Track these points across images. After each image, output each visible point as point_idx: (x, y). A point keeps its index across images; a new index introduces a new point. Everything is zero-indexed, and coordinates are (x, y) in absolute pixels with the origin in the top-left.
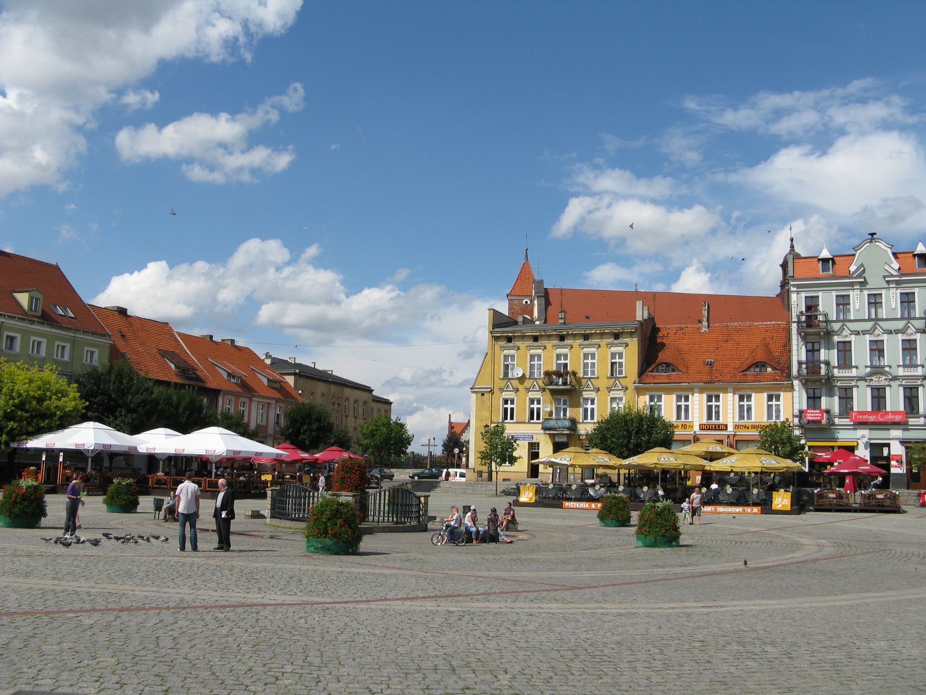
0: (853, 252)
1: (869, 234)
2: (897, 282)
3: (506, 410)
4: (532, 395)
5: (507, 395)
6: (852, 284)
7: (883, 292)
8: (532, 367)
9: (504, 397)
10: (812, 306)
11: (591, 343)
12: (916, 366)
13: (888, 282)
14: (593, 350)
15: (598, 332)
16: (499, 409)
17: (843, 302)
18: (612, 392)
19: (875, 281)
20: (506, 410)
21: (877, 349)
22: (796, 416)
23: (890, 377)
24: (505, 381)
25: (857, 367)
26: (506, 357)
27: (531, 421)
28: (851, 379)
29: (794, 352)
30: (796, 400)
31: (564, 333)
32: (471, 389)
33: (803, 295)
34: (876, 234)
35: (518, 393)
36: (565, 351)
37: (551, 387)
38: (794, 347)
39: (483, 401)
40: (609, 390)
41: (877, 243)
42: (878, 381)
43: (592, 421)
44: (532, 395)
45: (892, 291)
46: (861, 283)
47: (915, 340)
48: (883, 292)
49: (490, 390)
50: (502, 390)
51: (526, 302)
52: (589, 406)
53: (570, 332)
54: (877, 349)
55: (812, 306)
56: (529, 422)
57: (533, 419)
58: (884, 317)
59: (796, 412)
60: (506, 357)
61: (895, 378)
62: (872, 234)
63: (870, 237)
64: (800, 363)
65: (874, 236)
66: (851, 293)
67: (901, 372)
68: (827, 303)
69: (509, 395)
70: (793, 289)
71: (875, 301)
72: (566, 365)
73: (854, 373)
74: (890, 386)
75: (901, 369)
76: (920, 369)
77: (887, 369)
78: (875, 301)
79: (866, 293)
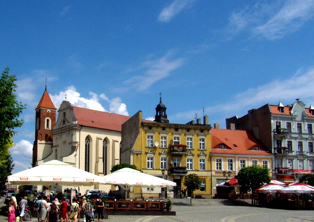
1: (296, 100)
2: (307, 119)
3: (148, 163)
10: (278, 126)
17: (289, 125)
20: (148, 163)
21: (300, 145)
28: (293, 156)
29: (273, 144)
30: (274, 164)
34: (299, 99)
36: (178, 136)
38: (273, 142)
39: (138, 158)
40: (199, 156)
43: (191, 170)
54: (300, 145)
55: (278, 126)
62: (297, 100)
63: (297, 100)
65: (299, 100)
67: (308, 155)
68: (284, 125)
69: (151, 155)
71: (299, 126)
72: (178, 142)
73: (294, 154)
77: (304, 153)
79: (296, 122)
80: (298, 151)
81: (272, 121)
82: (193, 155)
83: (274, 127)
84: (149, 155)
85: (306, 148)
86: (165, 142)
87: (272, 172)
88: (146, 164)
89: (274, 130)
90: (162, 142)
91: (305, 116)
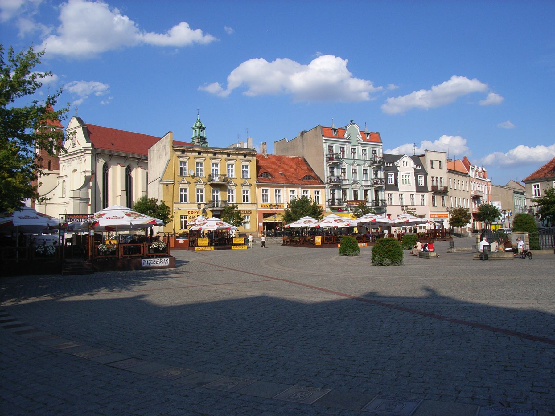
0: (345, 128)
4: (198, 186)
5: (182, 186)
6: (346, 142)
7: (356, 147)
8: (197, 169)
9: (181, 187)
11: (231, 158)
12: (368, 181)
13: (358, 143)
14: (232, 162)
15: (237, 152)
16: (178, 195)
18: (243, 187)
19: (354, 142)
22: (327, 202)
23: (360, 185)
24: (181, 178)
25: (348, 180)
26: (181, 163)
27: (181, 202)
28: (346, 185)
29: (325, 171)
31: (218, 151)
32: (161, 181)
33: (328, 145)
35: (190, 185)
37: (211, 183)
38: (325, 169)
40: (242, 185)
41: (354, 125)
42: (356, 186)
44: (198, 186)
45: (359, 147)
46: (349, 142)
47: (345, 169)
48: (356, 147)
49: (173, 183)
50: (180, 183)
51: (53, 130)
52: (231, 194)
53: (222, 151)
56: (180, 203)
57: (182, 201)
58: (357, 159)
59: (327, 200)
60: (181, 163)
61: (362, 186)
62: (352, 121)
64: (328, 177)
65: (353, 122)
66: (345, 146)
67: (363, 183)
70: (324, 141)
73: (347, 182)
74: (359, 189)
75: (363, 182)
76: (369, 182)
77: (358, 181)
78: (353, 151)
79: (351, 147)
80: (352, 179)
81: (324, 145)
82: (236, 185)
83: (326, 152)
84: (182, 186)
85: (359, 176)
86: (201, 170)
87: (325, 204)
88: (178, 197)
89: (327, 155)
90: (197, 169)
91: (360, 141)
